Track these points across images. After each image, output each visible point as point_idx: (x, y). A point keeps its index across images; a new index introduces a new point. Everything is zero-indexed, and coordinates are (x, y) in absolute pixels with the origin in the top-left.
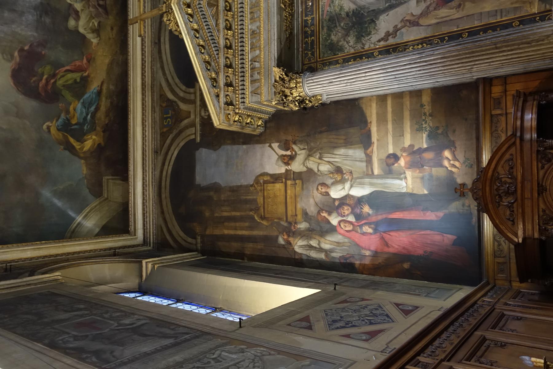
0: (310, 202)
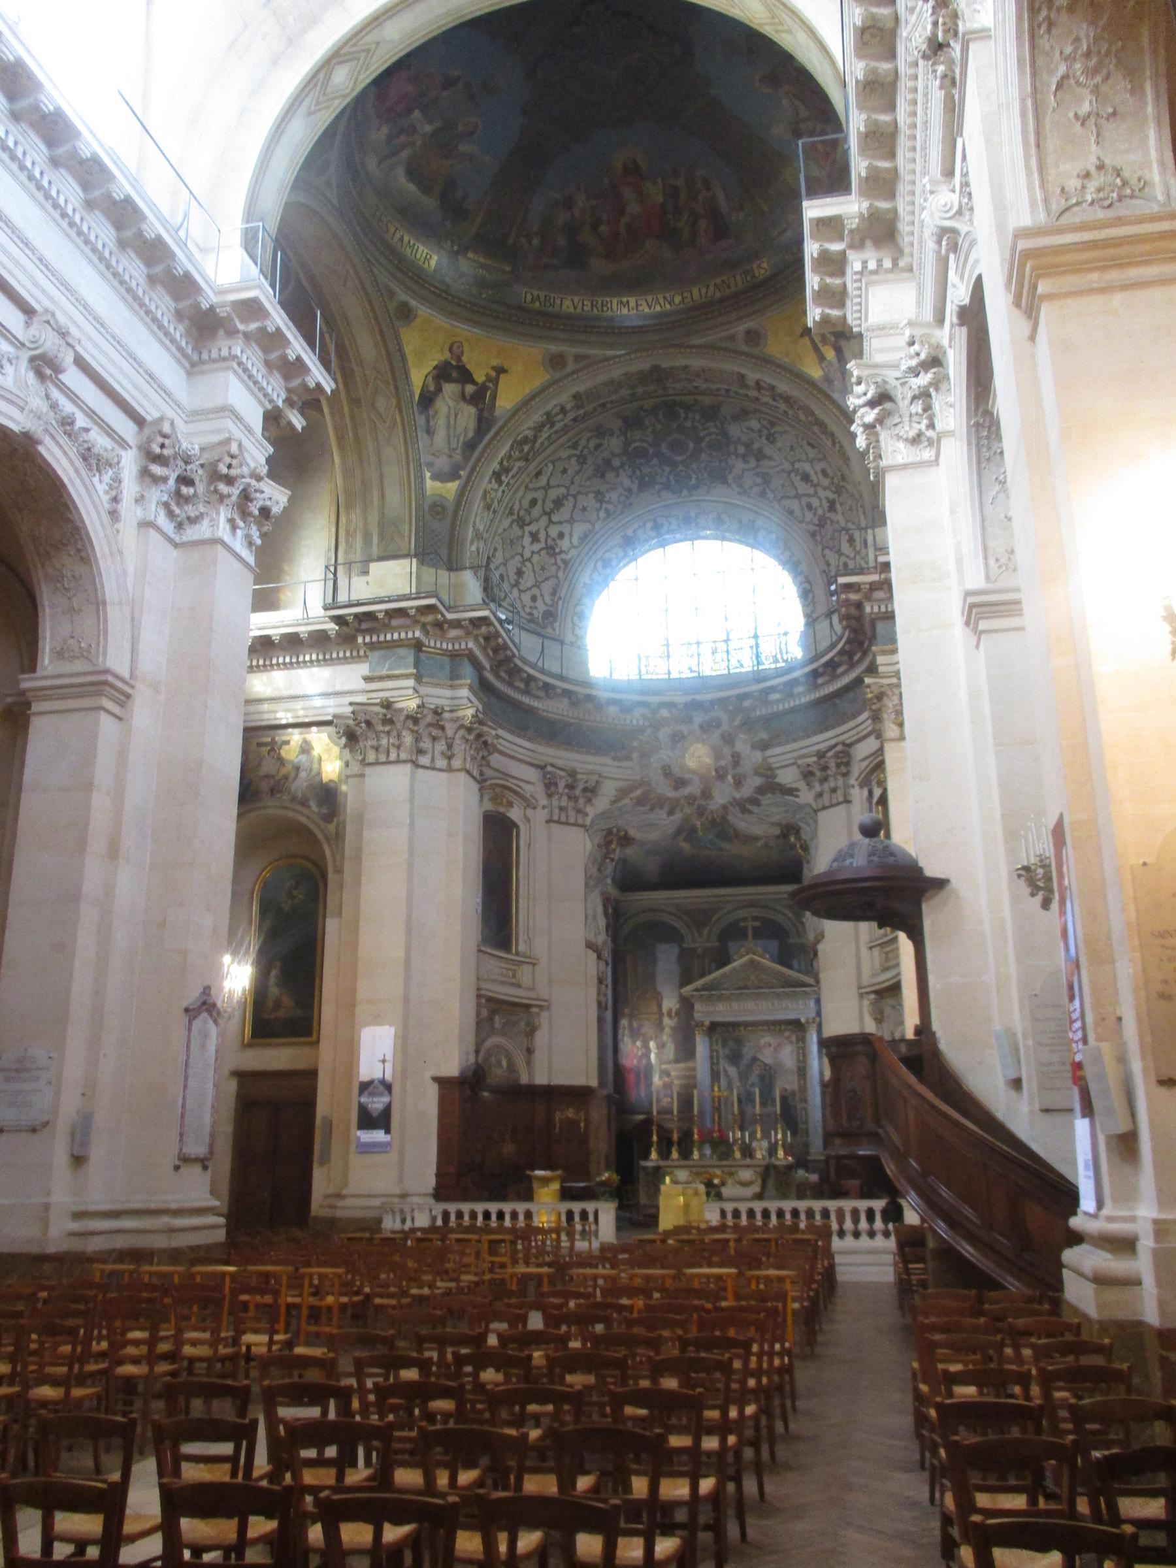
0: (648, 1028)
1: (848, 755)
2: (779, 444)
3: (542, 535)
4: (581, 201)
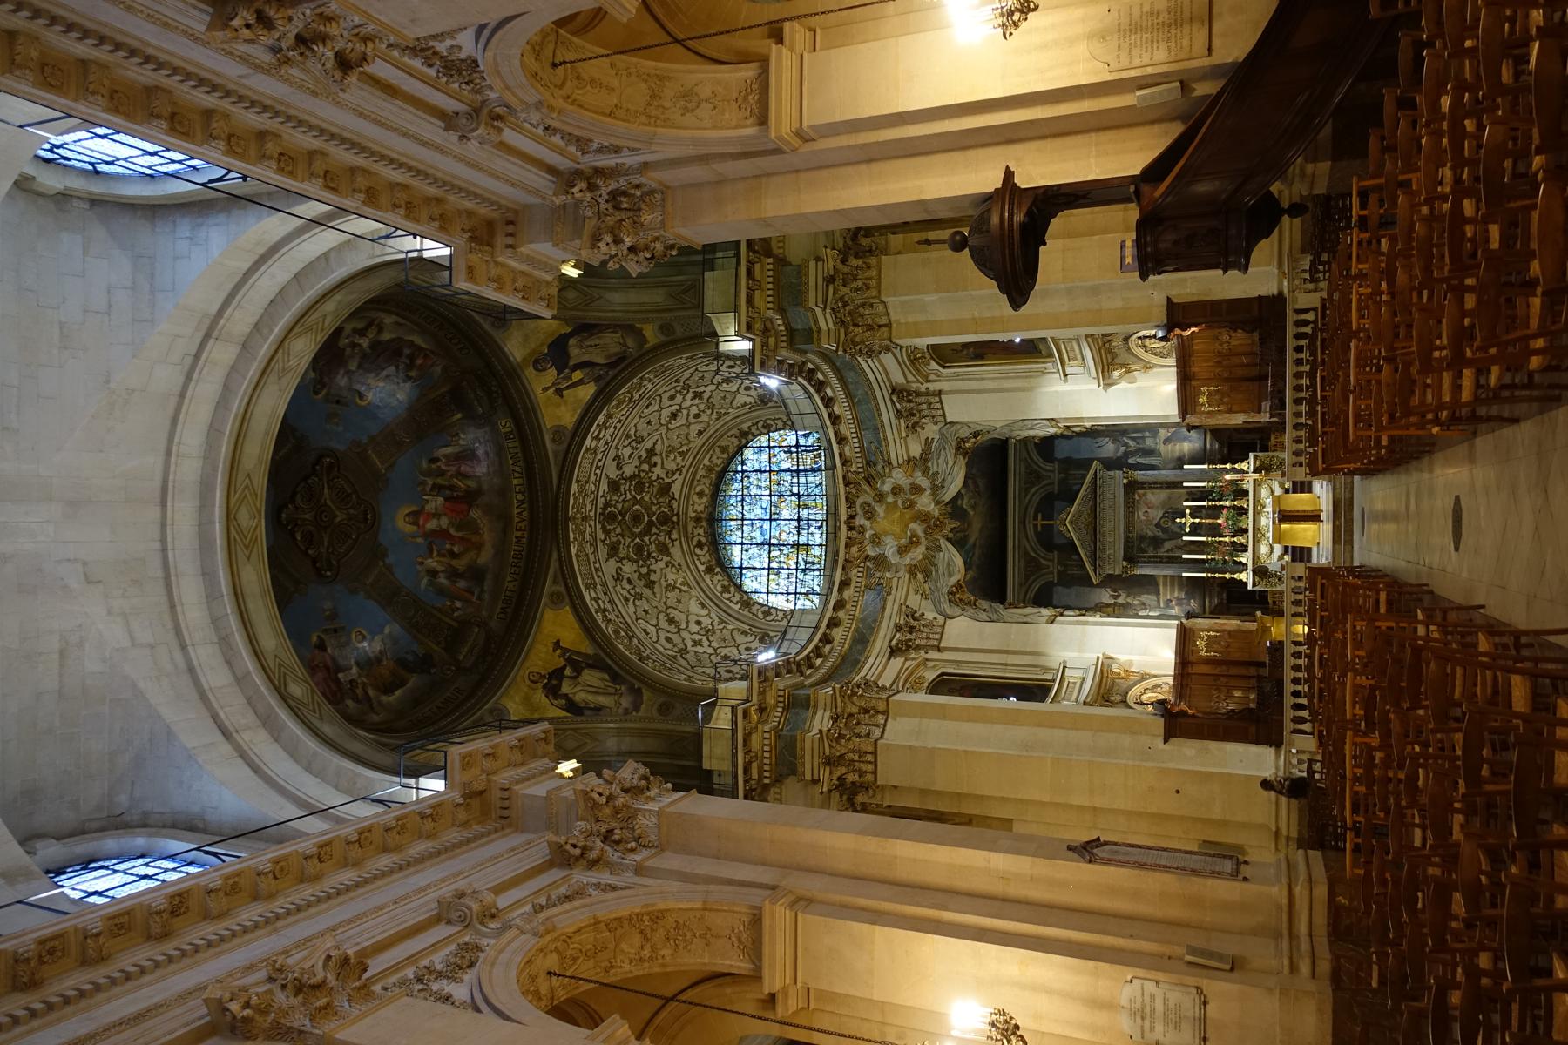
1: (901, 391)
2: (645, 434)
3: (697, 637)
4: (432, 563)
